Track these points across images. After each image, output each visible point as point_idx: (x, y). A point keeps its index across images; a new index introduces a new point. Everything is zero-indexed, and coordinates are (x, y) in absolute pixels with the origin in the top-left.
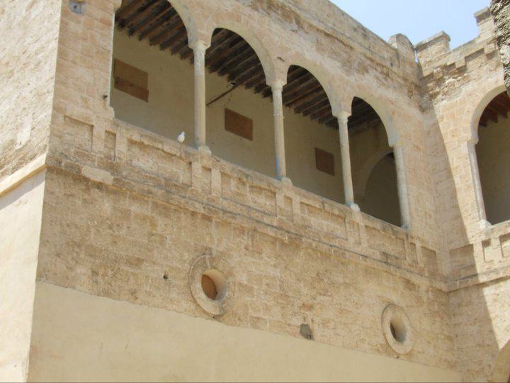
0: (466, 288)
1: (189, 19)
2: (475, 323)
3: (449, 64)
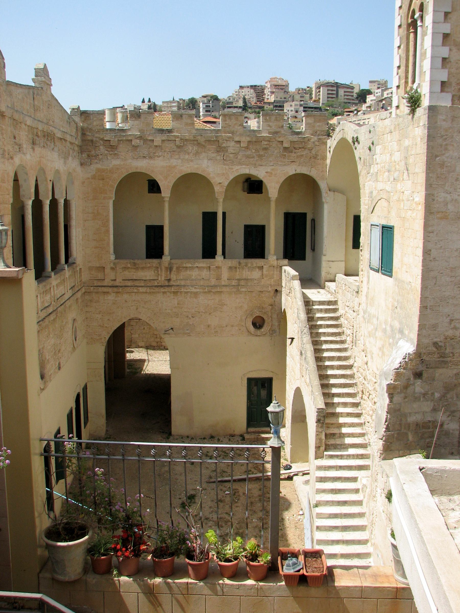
0: (97, 293)
1: (25, 180)
2: (100, 313)
3: (105, 139)
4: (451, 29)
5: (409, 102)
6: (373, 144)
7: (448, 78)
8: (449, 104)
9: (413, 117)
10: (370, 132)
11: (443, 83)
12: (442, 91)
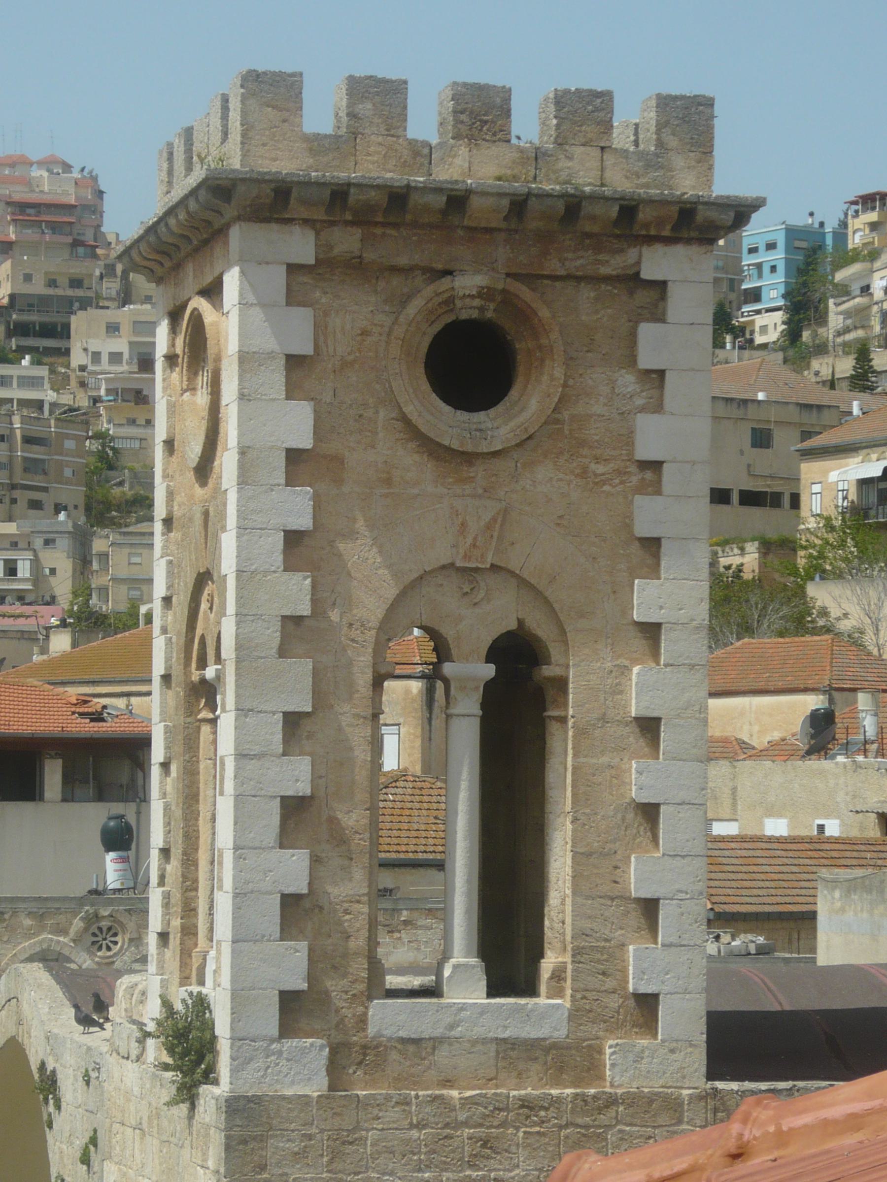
4: (316, 778)
5: (171, 1050)
6: (94, 1141)
7: (311, 978)
8: (315, 1086)
9: (191, 1117)
10: (88, 1083)
11: (289, 1002)
12: (287, 1030)
